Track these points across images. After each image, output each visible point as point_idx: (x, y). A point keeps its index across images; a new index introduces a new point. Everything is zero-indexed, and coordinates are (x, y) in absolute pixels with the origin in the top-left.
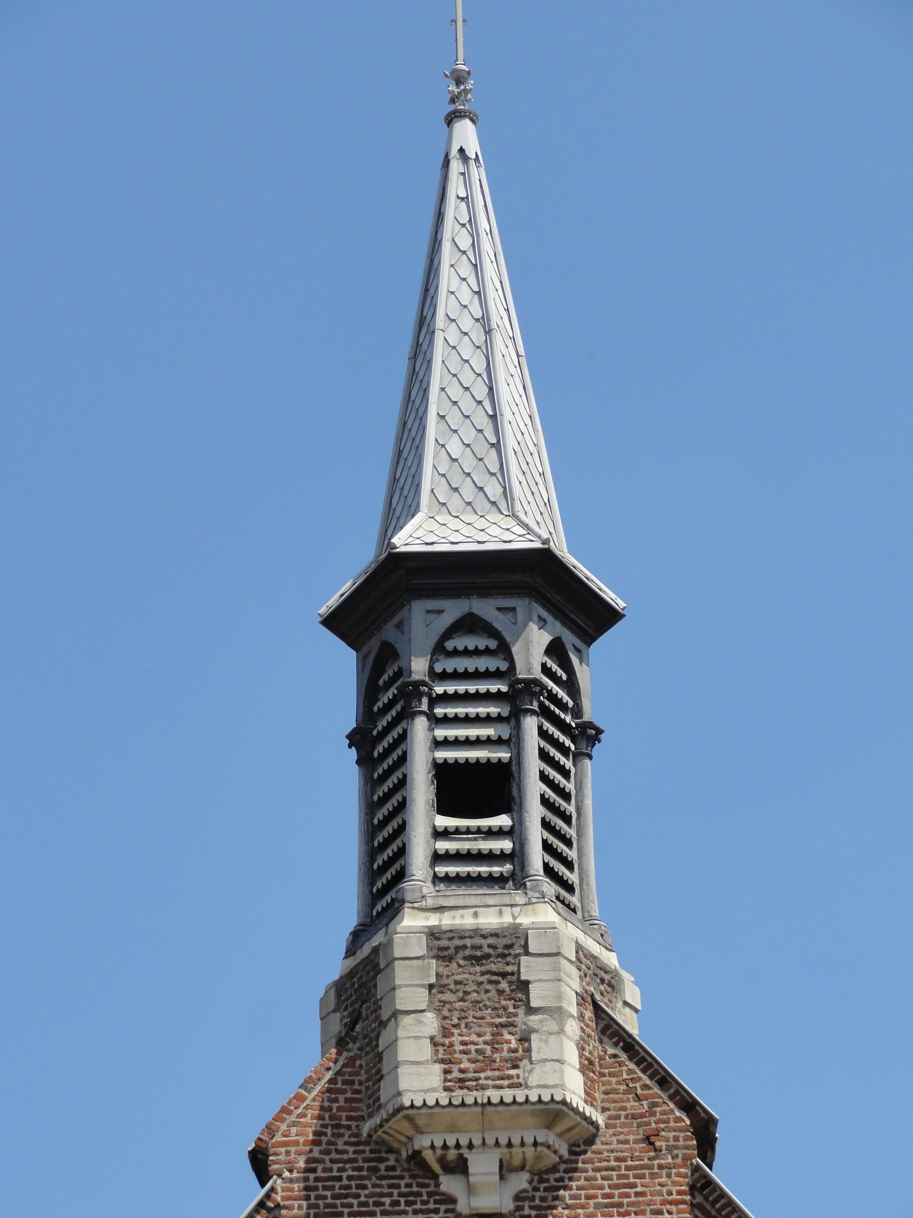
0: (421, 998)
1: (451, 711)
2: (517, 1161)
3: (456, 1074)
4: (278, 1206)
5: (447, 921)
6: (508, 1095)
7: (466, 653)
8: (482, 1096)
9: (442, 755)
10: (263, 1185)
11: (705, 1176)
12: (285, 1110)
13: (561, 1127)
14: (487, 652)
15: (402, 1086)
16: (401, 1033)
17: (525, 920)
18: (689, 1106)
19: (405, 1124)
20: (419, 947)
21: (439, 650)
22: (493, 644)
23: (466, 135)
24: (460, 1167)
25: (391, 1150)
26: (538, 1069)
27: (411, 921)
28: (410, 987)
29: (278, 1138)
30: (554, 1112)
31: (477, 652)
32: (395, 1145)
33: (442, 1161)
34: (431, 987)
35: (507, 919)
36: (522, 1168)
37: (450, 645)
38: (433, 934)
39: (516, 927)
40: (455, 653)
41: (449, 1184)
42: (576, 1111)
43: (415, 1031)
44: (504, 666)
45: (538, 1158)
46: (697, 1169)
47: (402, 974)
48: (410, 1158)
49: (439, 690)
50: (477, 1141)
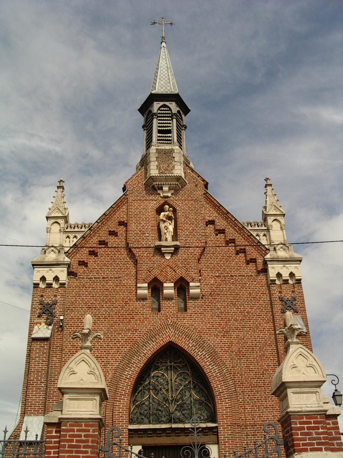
0: (155, 159)
1: (161, 118)
2: (172, 188)
3: (161, 171)
4: (127, 195)
5: (160, 148)
6: (171, 175)
7: (164, 110)
8: (166, 175)
9: (159, 128)
10: (124, 192)
11: (206, 191)
12: (129, 179)
13: (180, 182)
14: (167, 110)
15: (151, 173)
16: (151, 164)
17: (174, 148)
18: (204, 180)
19: (152, 180)
20: (155, 151)
21: (159, 109)
22: (168, 109)
23: (164, 44)
24: (161, 189)
25: (148, 186)
26: (176, 171)
27: (153, 150)
28: (153, 158)
29: (128, 184)
30: (178, 179)
31: (165, 110)
32: (149, 185)
33: (158, 187)
34: (157, 157)
35: (171, 147)
36: (173, 189)
37: (161, 109)
38: (157, 149)
39: (172, 149)
40: (162, 110)
41: (159, 191)
42: (182, 178)
43: (154, 164)
44: (170, 112)
45: (176, 187)
46: (205, 190)
47: (151, 155)
48: (152, 187)
49: (159, 115)
50: (165, 183)
